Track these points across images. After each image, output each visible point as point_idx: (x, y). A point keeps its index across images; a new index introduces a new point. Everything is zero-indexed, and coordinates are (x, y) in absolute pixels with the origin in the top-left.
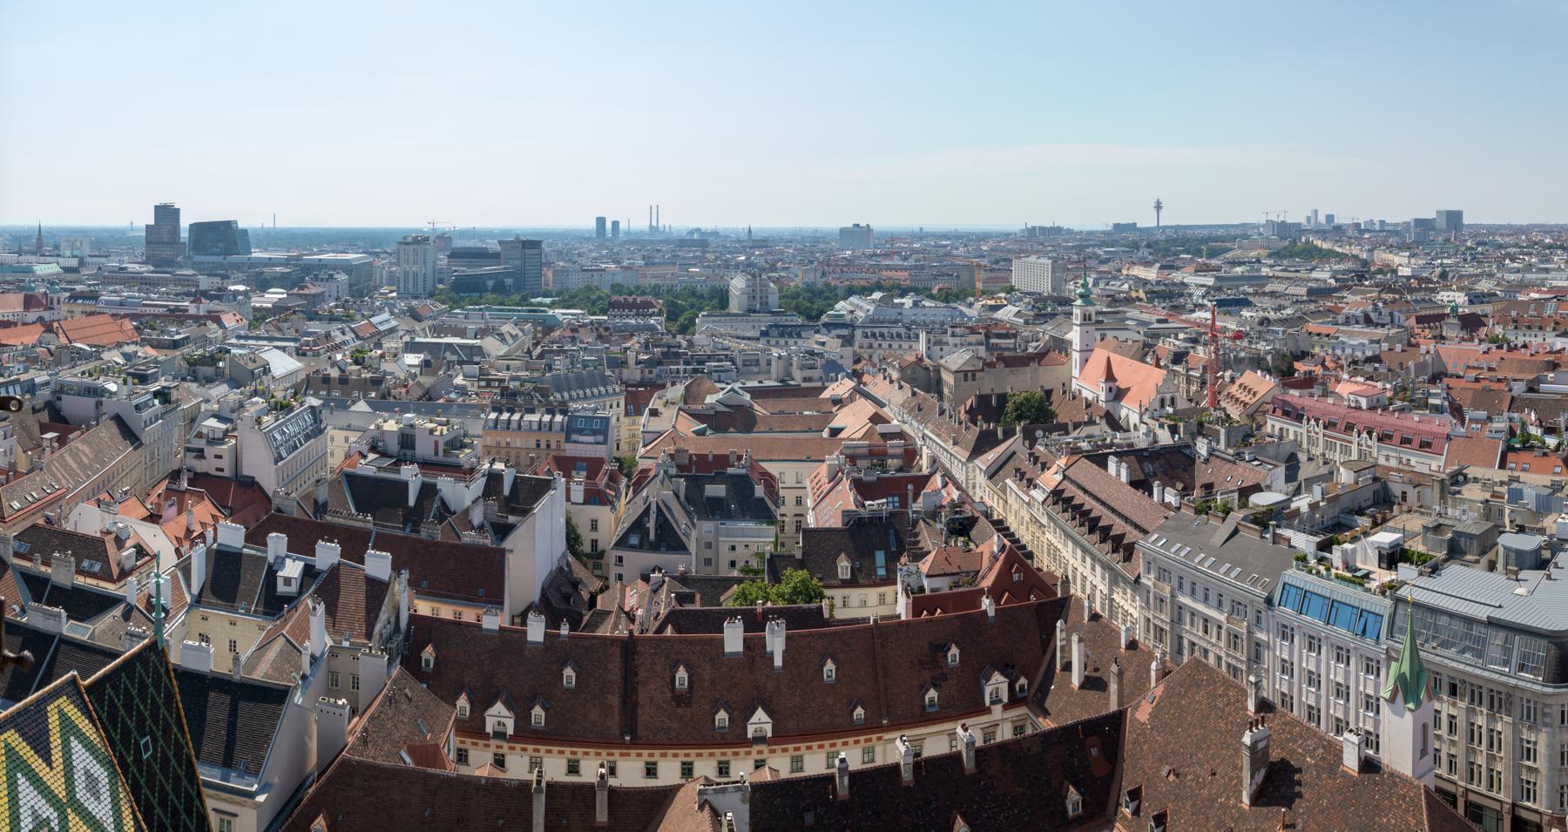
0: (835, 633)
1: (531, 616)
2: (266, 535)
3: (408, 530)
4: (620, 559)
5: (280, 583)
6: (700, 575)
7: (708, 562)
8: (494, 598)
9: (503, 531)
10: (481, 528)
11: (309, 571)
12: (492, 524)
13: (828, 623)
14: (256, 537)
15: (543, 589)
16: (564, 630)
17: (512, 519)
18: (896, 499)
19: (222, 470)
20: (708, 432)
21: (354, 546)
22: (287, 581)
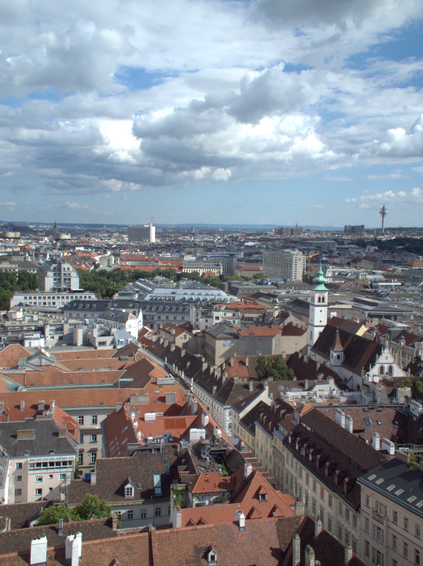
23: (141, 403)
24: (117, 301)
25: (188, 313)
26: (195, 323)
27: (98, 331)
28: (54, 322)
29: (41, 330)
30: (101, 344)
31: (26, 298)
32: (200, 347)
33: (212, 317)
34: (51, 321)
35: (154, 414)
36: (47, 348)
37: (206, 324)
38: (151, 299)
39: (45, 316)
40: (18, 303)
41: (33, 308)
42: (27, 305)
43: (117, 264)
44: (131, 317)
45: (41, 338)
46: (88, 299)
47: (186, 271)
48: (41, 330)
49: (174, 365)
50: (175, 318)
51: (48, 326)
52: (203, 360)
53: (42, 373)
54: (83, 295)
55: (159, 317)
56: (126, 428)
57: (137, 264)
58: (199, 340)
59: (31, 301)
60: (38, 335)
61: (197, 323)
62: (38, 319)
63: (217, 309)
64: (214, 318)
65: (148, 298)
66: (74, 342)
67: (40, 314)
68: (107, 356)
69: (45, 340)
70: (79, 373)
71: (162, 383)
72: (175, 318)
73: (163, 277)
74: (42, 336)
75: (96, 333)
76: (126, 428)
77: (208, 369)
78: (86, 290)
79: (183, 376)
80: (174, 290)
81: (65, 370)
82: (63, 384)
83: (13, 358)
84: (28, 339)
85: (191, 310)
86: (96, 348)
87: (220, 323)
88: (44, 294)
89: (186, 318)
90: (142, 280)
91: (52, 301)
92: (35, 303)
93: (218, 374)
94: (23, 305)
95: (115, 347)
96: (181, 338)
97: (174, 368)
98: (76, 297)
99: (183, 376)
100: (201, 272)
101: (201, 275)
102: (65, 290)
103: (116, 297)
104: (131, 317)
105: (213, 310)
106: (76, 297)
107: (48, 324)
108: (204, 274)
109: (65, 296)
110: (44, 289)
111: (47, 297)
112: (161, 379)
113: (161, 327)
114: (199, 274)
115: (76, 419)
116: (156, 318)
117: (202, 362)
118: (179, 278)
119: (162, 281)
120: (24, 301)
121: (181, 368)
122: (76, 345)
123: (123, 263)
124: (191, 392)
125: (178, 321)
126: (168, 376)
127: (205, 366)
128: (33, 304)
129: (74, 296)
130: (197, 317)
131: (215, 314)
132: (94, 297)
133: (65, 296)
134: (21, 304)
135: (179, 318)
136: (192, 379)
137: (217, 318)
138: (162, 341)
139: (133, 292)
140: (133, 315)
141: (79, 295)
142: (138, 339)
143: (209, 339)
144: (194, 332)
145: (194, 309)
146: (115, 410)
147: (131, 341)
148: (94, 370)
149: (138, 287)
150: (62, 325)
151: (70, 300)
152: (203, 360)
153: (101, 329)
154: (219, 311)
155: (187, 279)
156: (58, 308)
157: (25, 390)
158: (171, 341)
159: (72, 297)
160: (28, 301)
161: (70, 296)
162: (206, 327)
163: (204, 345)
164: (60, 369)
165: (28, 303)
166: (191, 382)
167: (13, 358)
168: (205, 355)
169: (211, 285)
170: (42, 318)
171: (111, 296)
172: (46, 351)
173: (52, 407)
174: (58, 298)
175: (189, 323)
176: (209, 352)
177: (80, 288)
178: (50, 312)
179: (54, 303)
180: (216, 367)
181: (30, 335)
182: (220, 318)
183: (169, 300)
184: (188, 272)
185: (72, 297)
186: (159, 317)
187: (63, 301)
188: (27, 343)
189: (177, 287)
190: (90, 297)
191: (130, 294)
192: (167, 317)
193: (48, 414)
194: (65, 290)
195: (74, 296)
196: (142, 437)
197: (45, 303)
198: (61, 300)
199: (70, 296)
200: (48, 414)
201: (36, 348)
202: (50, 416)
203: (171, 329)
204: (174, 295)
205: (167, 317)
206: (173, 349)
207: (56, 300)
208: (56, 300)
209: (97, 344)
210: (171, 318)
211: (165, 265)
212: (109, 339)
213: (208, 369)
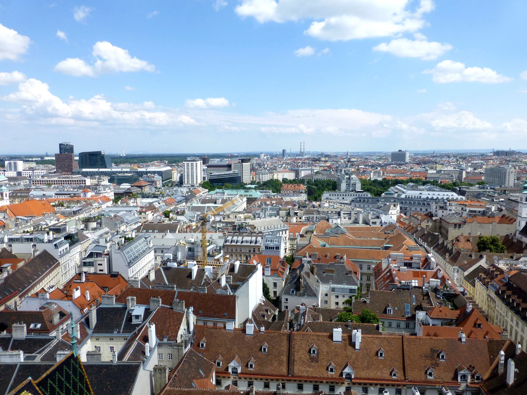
1: (247, 324)
2: (125, 298)
3: (192, 290)
4: (287, 300)
5: (133, 318)
6: (323, 308)
7: (326, 302)
8: (232, 317)
9: (235, 288)
10: (225, 288)
11: (147, 312)
12: (230, 285)
14: (121, 299)
15: (253, 312)
16: (263, 329)
17: (238, 283)
18: (416, 281)
19: (102, 270)
20: (327, 245)
21: (168, 298)
22: (137, 317)
24: (384, 198)
29: (339, 214)
30: (373, 223)
31: (330, 195)
37: (443, 214)
39: (341, 205)
40: (326, 198)
61: (436, 213)
64: (448, 210)
65: (403, 196)
67: (338, 204)
72: (421, 209)
77: (443, 243)
78: (365, 191)
80: (421, 192)
83: (322, 228)
90: (400, 185)
93: (449, 246)
96: (425, 222)
106: (359, 195)
116: (408, 209)
119: (412, 186)
121: (424, 241)
132: (369, 195)
134: (327, 199)
137: (450, 210)
142: (397, 221)
144: (434, 218)
151: (355, 197)
153: (374, 214)
159: (356, 195)
162: (443, 216)
163: (441, 227)
168: (441, 233)
178: (344, 204)
185: (356, 195)
186: (411, 209)
188: (330, 220)
190: (367, 195)
191: (392, 194)
192: (416, 209)
194: (352, 191)
201: (335, 224)
202: (343, 263)
205: (416, 209)
212: (378, 221)
213: (443, 243)
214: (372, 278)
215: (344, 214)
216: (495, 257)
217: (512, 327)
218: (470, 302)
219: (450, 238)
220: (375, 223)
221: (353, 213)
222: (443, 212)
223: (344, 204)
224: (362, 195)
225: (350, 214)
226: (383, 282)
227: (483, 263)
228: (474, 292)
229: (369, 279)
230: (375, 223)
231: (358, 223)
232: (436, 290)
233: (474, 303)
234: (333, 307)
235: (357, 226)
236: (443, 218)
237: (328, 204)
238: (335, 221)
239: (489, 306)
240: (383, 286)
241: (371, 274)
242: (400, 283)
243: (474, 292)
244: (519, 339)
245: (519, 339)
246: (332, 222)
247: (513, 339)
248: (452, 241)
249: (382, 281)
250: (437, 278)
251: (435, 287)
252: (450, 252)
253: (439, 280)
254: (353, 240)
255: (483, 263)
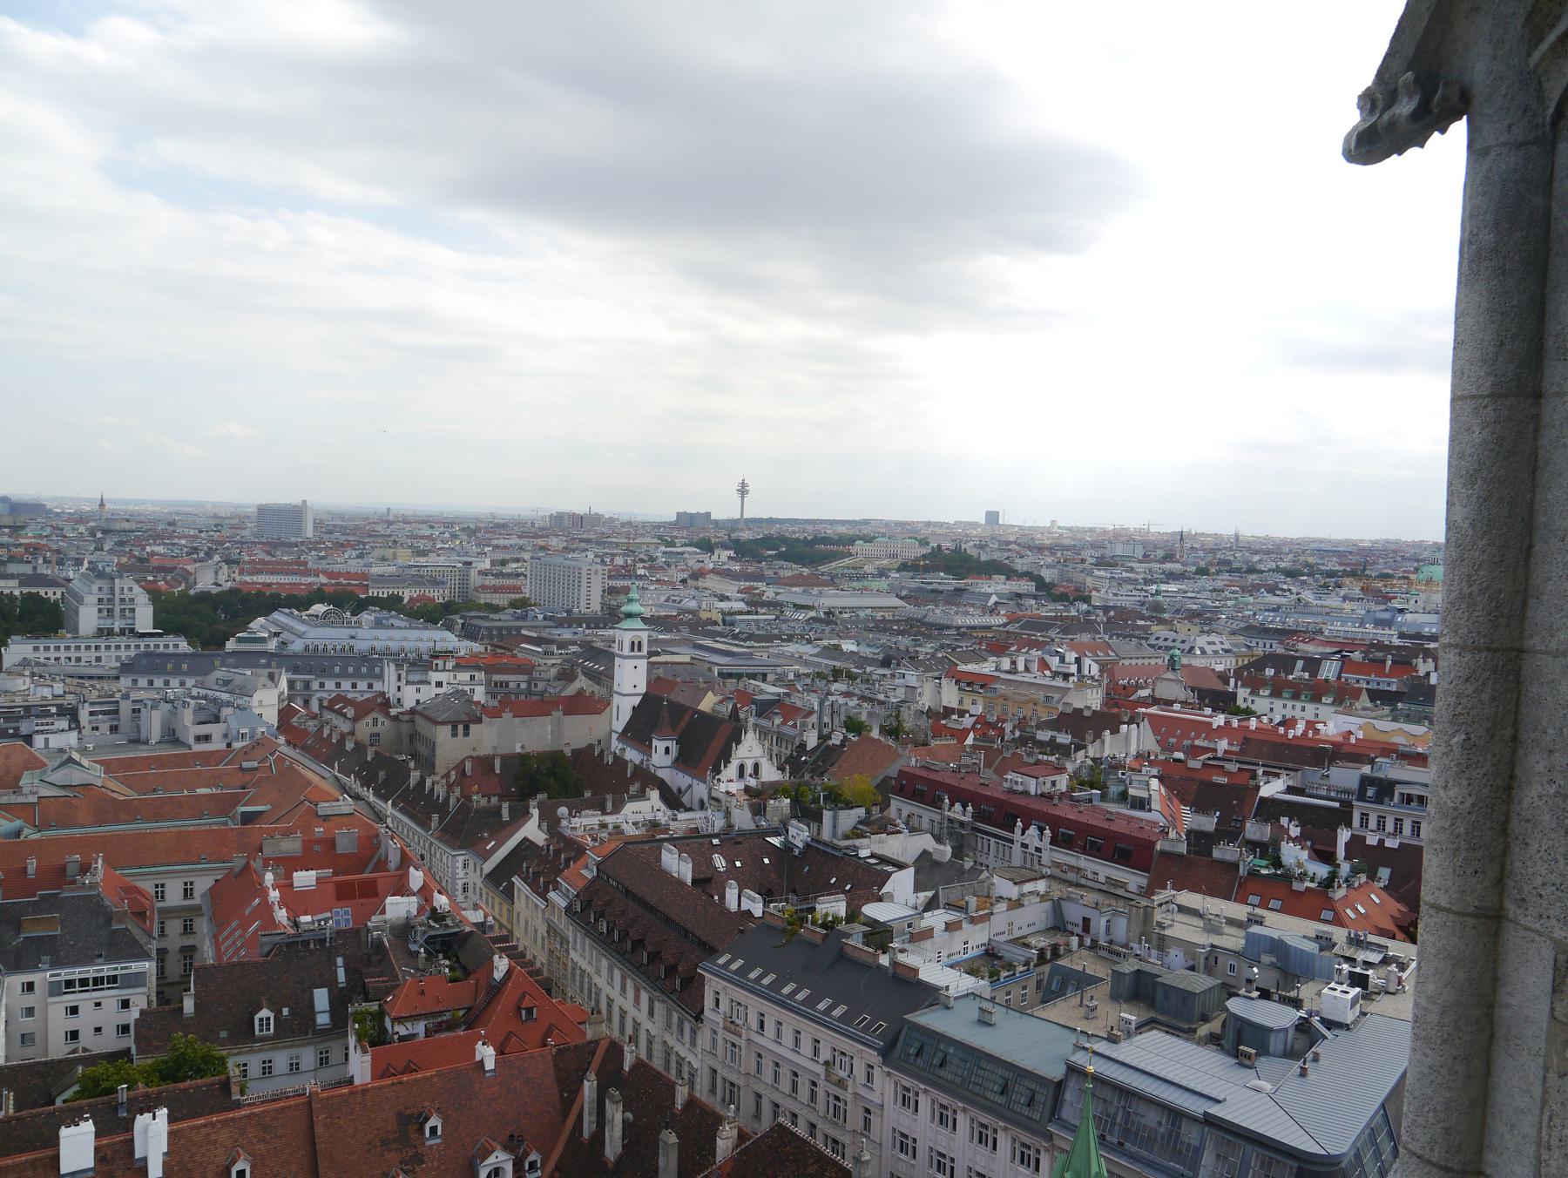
0: (249, 1117)
7: (26, 1039)
13: (237, 1105)
20: (26, 831)
23: (286, 852)
24: (234, 653)
25: (380, 677)
26: (394, 695)
27: (195, 712)
28: (99, 697)
29: (72, 714)
30: (198, 739)
31: (36, 649)
32: (406, 741)
33: (430, 683)
34: (93, 697)
35: (313, 873)
36: (83, 751)
37: (418, 696)
38: (307, 648)
39: (79, 685)
40: (17, 659)
41: (53, 670)
42: (38, 664)
43: (234, 580)
44: (264, 686)
45: (70, 729)
46: (171, 650)
47: (375, 594)
48: (72, 714)
49: (352, 777)
50: (354, 686)
51: (87, 705)
52: (412, 764)
53: (74, 801)
54: (161, 642)
55: (322, 685)
56: (257, 901)
57: (274, 581)
58: (405, 728)
59: (47, 655)
60: (63, 723)
61: (399, 695)
62: (65, 692)
63: (441, 667)
64: (434, 684)
65: (297, 646)
66: (143, 737)
67: (68, 680)
68: (213, 763)
69: (80, 732)
70: (154, 799)
71: (328, 813)
72: (354, 686)
73: (329, 605)
74: (73, 726)
75: (188, 716)
76: (257, 901)
77: (422, 782)
78: (167, 632)
79: (372, 798)
80: (353, 632)
81: (122, 792)
82: (120, 821)
83: (8, 772)
84: (42, 732)
85: (386, 669)
86: (189, 747)
87: (445, 694)
88: (77, 640)
89: (377, 686)
90: (287, 610)
91: (93, 654)
92: (57, 659)
93: (440, 791)
94: (28, 665)
95: (229, 745)
96: (367, 725)
97: (350, 781)
98: (147, 646)
99: (372, 798)
100: (407, 594)
101: (406, 601)
102: (122, 632)
103: (231, 645)
104: (264, 686)
105: (431, 669)
106: (147, 646)
107: (85, 702)
108: (411, 600)
109: (123, 645)
110: (76, 630)
111: (83, 646)
112: (326, 804)
113: (325, 704)
114: (402, 599)
115: (150, 891)
116: (315, 686)
117: (410, 770)
118: (360, 606)
119: (326, 614)
120: (31, 656)
121: (366, 783)
122: (146, 743)
123: (248, 579)
124: (387, 827)
125: (360, 691)
126: (341, 798)
127: (415, 776)
128: (52, 661)
129: (142, 645)
130: (399, 684)
131: (435, 677)
132: (183, 646)
133: (123, 645)
134: (25, 663)
135: (362, 685)
136: (390, 802)
137: (439, 684)
138: (326, 732)
139: (266, 635)
140: (269, 683)
141: (152, 642)
142: (278, 728)
143: (422, 725)
144: (393, 712)
145: (392, 666)
146: (231, 869)
147: (263, 732)
148: (186, 792)
149: (275, 623)
150: (117, 702)
151: (132, 653)
152: (412, 764)
153: (200, 708)
154: (444, 670)
155: (377, 609)
156: (107, 668)
157: (37, 836)
158: (346, 731)
159: (138, 647)
160: (42, 655)
161: (133, 645)
162: (418, 702)
163: (414, 737)
164: (113, 791)
165: (42, 660)
166: (388, 808)
167: (8, 772)
168: (414, 756)
169: (427, 621)
170: (72, 689)
171: (222, 645)
172: (82, 755)
173: (96, 868)
174: (108, 648)
175: (383, 694)
176: (423, 750)
177: (154, 628)
178: (91, 678)
179: (99, 659)
180: (437, 778)
181: (47, 724)
182: (444, 684)
183: (343, 650)
184: (380, 595)
185: (138, 647)
186: (322, 685)
187: (119, 654)
188: (39, 741)
189: (359, 624)
190: (176, 646)
191: (263, 640)
192: (338, 685)
193: (87, 882)
194: (122, 632)
195: (142, 645)
196: (289, 919)
197: (78, 659)
198: (113, 653)
199: (133, 645)
200: (87, 882)
201: (61, 751)
202: (93, 886)
203: (344, 707)
204: (353, 641)
205: (338, 685)
206: (349, 746)
207: (103, 653)
208: (103, 653)
209: (191, 740)
210: (346, 685)
211: (333, 581)
212: (215, 730)
213: (422, 782)
214: (203, 926)
215: (92, 714)
216: (563, 811)
217: (610, 1002)
218: (502, 950)
219: (441, 767)
220: (207, 738)
221: (126, 707)
222: (418, 690)
223: (91, 678)
224: (157, 646)
225: (116, 712)
226: (238, 933)
227: (532, 830)
228: (510, 920)
229: (188, 929)
230: (207, 738)
231: (146, 743)
232: (404, 930)
233: (515, 954)
234: (58, 1049)
235: (142, 752)
236: (419, 708)
237: (28, 680)
238: (56, 741)
239: (551, 952)
240: (239, 944)
241: (197, 910)
242: (296, 924)
243: (510, 920)
244: (629, 1030)
245: (629, 1030)
246: (47, 746)
247: (616, 1034)
248: (447, 776)
249: (236, 929)
250: (409, 893)
251: (402, 921)
252: (442, 808)
253: (414, 899)
254: (127, 804)
255: (532, 830)
